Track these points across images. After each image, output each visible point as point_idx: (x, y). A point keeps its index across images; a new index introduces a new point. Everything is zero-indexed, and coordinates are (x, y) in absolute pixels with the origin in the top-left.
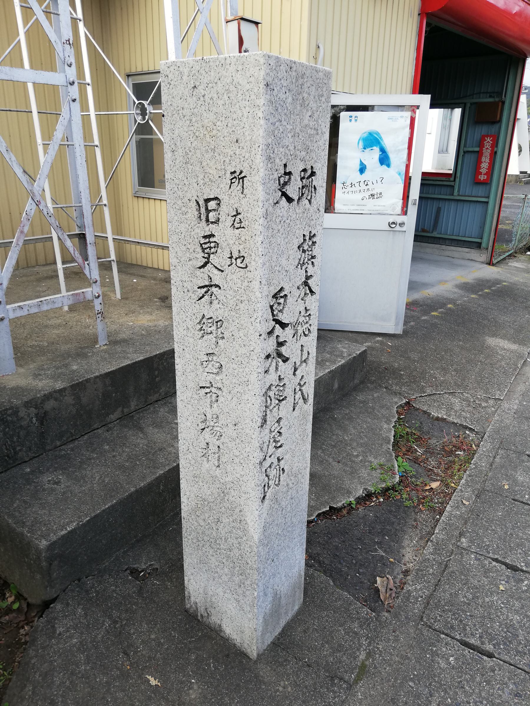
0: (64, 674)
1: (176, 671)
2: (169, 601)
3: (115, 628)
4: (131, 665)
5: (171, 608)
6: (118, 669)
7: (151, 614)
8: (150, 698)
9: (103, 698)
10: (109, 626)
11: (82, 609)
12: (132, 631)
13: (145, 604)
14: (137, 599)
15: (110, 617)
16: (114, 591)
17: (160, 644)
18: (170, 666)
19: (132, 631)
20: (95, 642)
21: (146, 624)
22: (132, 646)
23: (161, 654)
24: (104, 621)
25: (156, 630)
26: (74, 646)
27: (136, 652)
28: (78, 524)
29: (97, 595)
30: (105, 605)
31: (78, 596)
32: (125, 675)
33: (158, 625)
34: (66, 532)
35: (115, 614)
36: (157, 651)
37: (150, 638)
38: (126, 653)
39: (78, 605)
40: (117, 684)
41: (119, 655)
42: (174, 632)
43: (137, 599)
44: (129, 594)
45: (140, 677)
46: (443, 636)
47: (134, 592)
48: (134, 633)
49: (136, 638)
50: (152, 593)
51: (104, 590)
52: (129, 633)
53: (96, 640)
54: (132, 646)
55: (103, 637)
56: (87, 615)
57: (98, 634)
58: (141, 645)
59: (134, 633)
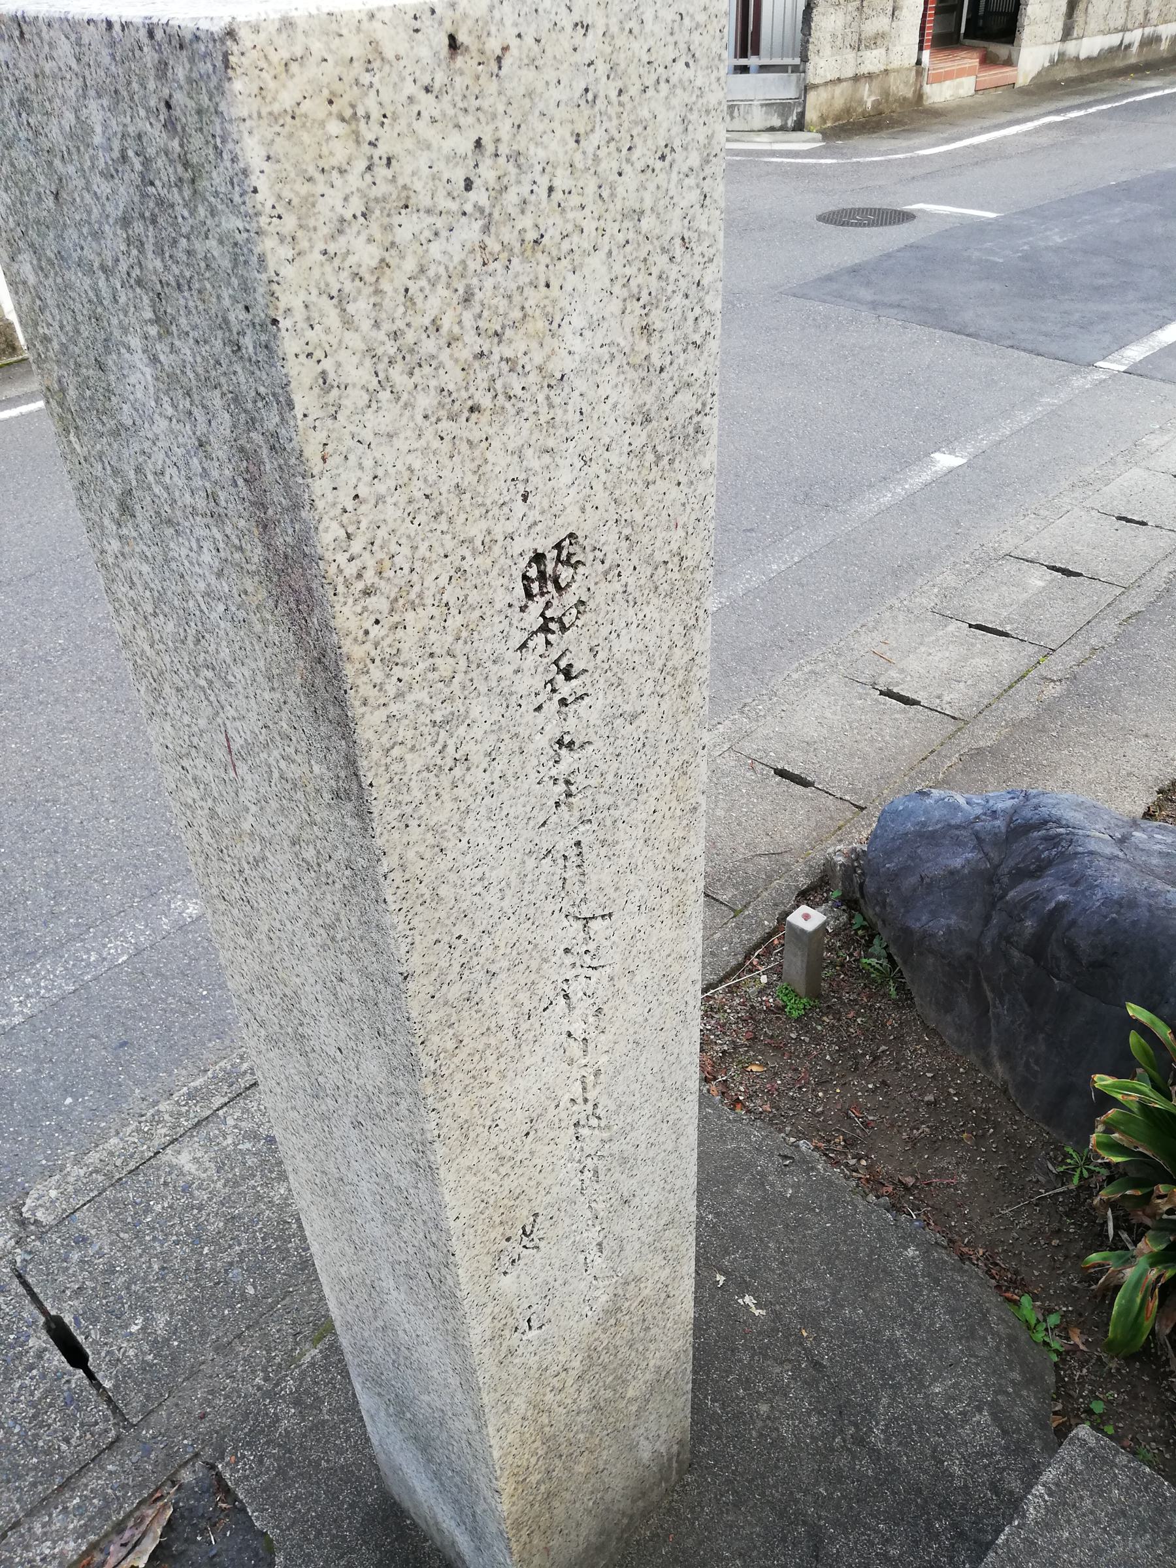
0: (933, 1324)
1: (706, 1323)
2: (736, 1505)
3: (856, 1425)
4: (800, 1340)
5: (729, 1482)
6: (826, 1331)
7: (777, 1467)
8: (753, 1274)
9: (841, 1280)
10: (871, 1430)
11: (952, 1475)
12: (814, 1419)
13: (796, 1501)
14: (820, 1517)
15: (874, 1452)
16: (887, 1542)
17: (747, 1383)
18: (718, 1334)
19: (814, 1419)
20: (892, 1386)
21: (784, 1438)
22: (805, 1382)
23: (740, 1360)
24: (887, 1441)
25: (760, 1424)
26: (934, 1379)
27: (796, 1369)
28: (1024, 1516)
29: (929, 1525)
30: (898, 1493)
31: (979, 1519)
32: (811, 1319)
33: (754, 1433)
34: (1043, 1478)
35: (865, 1466)
36: (751, 1367)
37: (770, 1401)
38: (817, 1365)
39: (966, 1486)
40: (819, 1303)
41: (830, 1359)
42: (715, 1412)
43: (820, 1517)
44: (845, 1533)
45: (777, 1316)
46: (107, 1384)
47: (833, 1539)
48: (809, 1413)
49: (802, 1400)
50: (784, 1539)
51: (916, 1543)
52: (820, 1413)
53: (890, 1392)
54: (805, 1382)
55: (877, 1400)
56: (933, 1457)
57: (890, 1405)
58: (788, 1385)
59: (809, 1413)
